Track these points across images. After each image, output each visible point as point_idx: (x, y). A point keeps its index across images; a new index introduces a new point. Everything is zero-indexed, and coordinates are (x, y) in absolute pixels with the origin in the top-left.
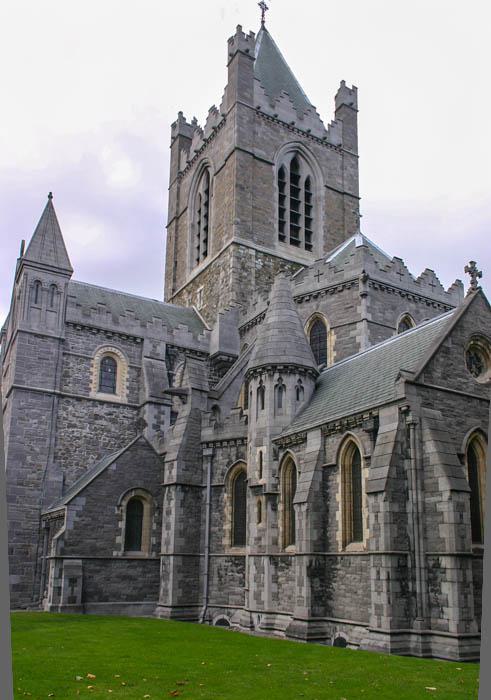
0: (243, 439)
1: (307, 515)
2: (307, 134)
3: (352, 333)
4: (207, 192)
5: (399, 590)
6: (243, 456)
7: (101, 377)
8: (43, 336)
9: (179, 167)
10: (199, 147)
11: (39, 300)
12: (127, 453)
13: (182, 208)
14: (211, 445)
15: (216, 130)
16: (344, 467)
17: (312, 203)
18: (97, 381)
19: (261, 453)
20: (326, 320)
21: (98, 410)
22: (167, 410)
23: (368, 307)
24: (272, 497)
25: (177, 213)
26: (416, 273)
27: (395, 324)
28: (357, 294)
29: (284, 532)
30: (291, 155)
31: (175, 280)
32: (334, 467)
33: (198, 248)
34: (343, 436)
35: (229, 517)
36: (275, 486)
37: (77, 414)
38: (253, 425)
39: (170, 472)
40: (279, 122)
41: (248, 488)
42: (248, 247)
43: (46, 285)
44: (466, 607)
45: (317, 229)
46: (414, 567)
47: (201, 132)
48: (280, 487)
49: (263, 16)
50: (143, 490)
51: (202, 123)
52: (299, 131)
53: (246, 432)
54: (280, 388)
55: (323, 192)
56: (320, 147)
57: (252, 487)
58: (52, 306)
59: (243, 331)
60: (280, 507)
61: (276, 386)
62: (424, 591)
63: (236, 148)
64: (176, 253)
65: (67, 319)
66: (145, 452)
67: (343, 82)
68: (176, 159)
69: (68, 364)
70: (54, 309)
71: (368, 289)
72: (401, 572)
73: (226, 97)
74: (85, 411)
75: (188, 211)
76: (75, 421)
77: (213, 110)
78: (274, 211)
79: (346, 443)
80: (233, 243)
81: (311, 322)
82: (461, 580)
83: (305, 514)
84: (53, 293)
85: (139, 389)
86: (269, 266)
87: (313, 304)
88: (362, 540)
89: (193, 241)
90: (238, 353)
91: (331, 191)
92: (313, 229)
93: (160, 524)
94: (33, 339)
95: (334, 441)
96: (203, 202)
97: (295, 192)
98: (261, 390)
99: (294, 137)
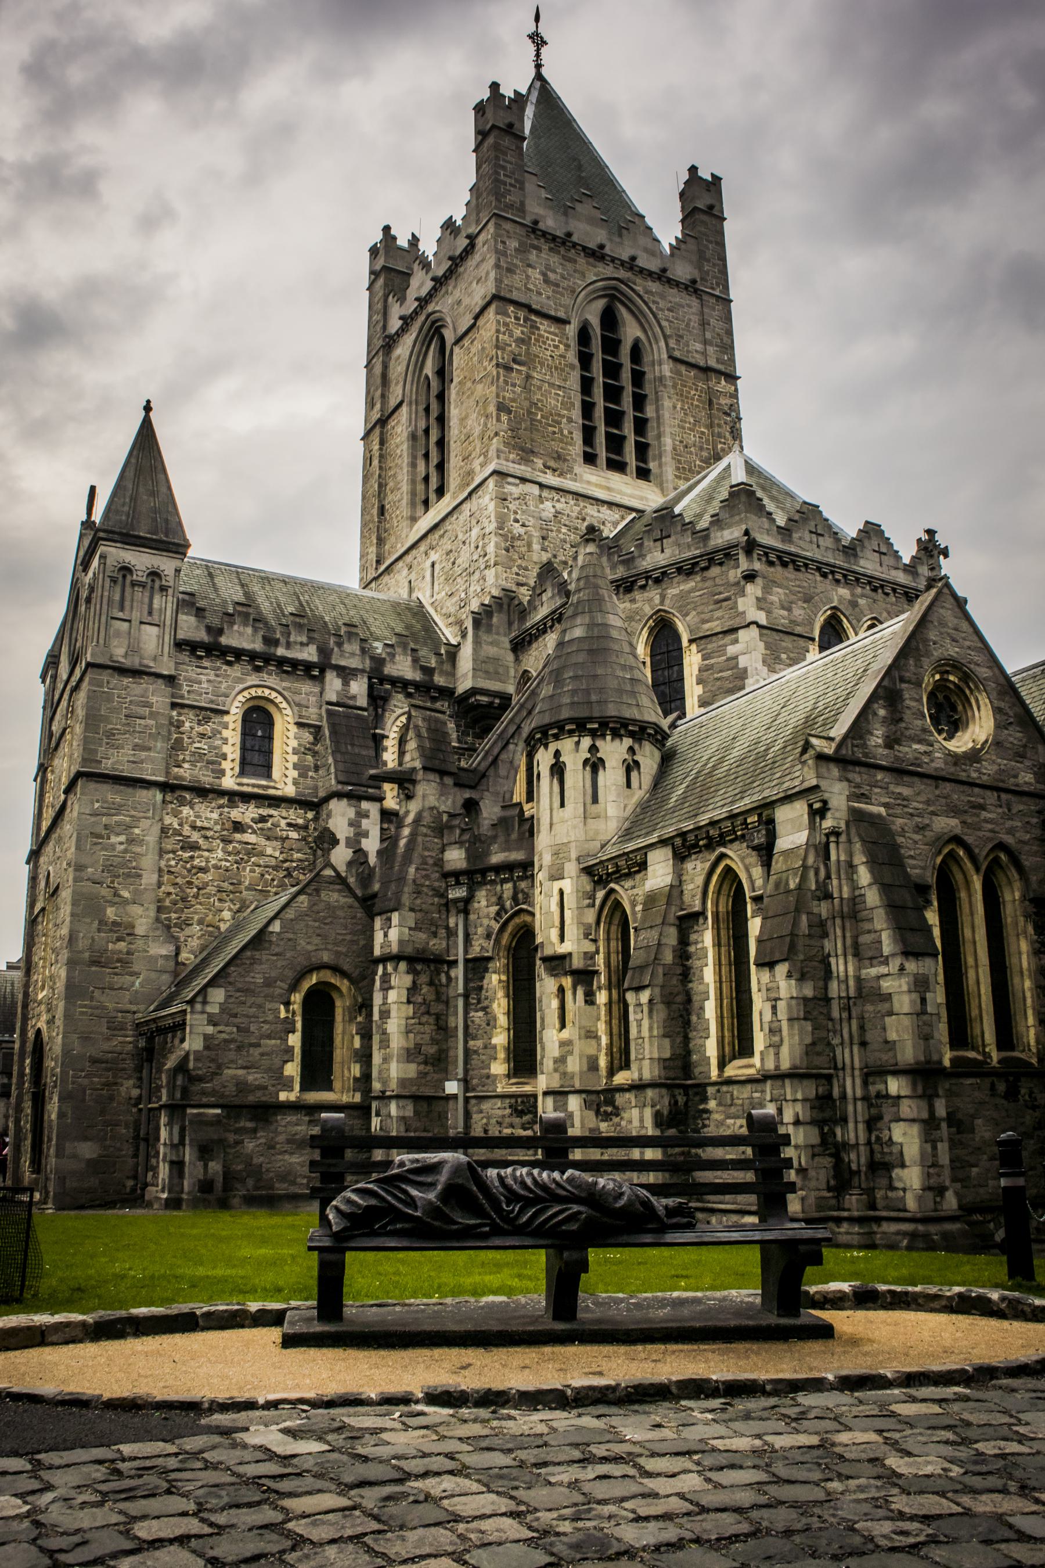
0: (527, 867)
1: (651, 1011)
2: (631, 264)
3: (731, 650)
5: (815, 1140)
6: (528, 898)
7: (243, 749)
8: (137, 673)
9: (385, 327)
10: (423, 292)
11: (127, 604)
12: (302, 898)
13: (393, 403)
14: (463, 879)
15: (457, 261)
16: (716, 915)
17: (648, 389)
18: (237, 755)
19: (561, 893)
20: (681, 627)
21: (235, 814)
22: (372, 808)
23: (758, 599)
24: (584, 977)
26: (850, 530)
27: (812, 630)
28: (734, 574)
29: (610, 1046)
30: (600, 304)
31: (381, 541)
33: (426, 479)
34: (713, 857)
35: (502, 1020)
36: (590, 956)
37: (199, 824)
38: (543, 841)
39: (386, 935)
40: (574, 245)
41: (538, 962)
42: (524, 480)
43: (140, 576)
44: (934, 1165)
45: (659, 436)
46: (843, 1096)
47: (426, 265)
48: (600, 959)
50: (336, 969)
51: (428, 247)
52: (613, 260)
53: (531, 849)
54: (595, 765)
55: (667, 369)
56: (654, 286)
57: (545, 960)
58: (150, 613)
59: (520, 646)
60: (602, 997)
61: (586, 762)
62: (862, 1140)
63: (495, 297)
65: (181, 635)
66: (335, 896)
67: (693, 170)
68: (378, 312)
69: (179, 725)
70: (156, 619)
71: (757, 566)
72: (821, 1109)
73: (474, 202)
74: (215, 816)
75: (404, 409)
76: (195, 836)
77: (449, 226)
79: (719, 870)
80: (495, 472)
81: (651, 629)
82: (925, 1115)
83: (646, 1009)
84: (152, 588)
85: (317, 768)
87: (654, 594)
88: (750, 1053)
89: (413, 465)
90: (511, 689)
91: (683, 369)
92: (651, 437)
93: (366, 1036)
94: (116, 680)
95: (697, 868)
96: (434, 391)
97: (612, 370)
98: (558, 770)
99: (609, 271)
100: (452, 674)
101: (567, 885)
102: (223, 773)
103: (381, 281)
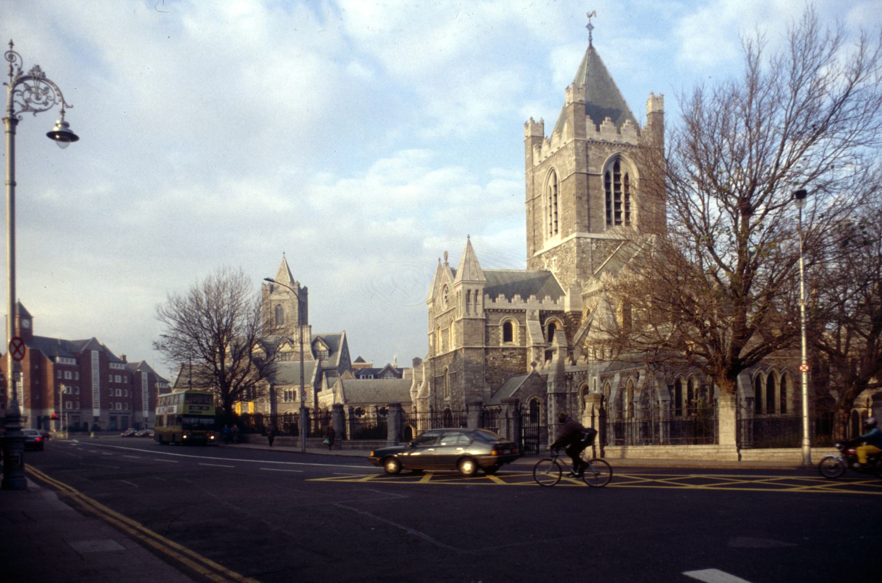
4: (555, 186)
21: (504, 353)
25: (533, 196)
32: (624, 389)
49: (590, 33)
59: (584, 297)
64: (534, 224)
78: (602, 207)
86: (600, 246)
95: (625, 379)
96: (553, 193)
100: (563, 306)
101: (596, 378)
102: (499, 342)
103: (530, 141)
